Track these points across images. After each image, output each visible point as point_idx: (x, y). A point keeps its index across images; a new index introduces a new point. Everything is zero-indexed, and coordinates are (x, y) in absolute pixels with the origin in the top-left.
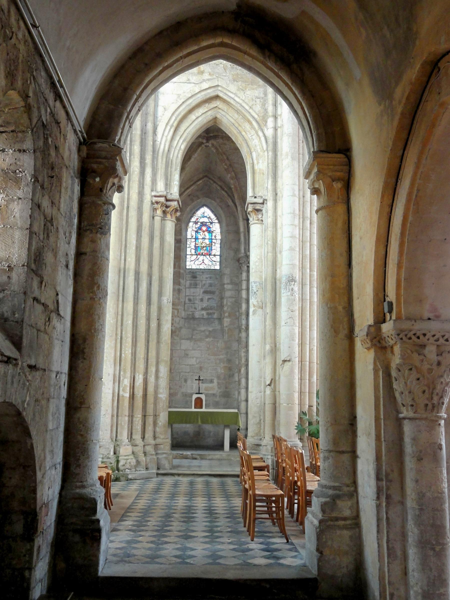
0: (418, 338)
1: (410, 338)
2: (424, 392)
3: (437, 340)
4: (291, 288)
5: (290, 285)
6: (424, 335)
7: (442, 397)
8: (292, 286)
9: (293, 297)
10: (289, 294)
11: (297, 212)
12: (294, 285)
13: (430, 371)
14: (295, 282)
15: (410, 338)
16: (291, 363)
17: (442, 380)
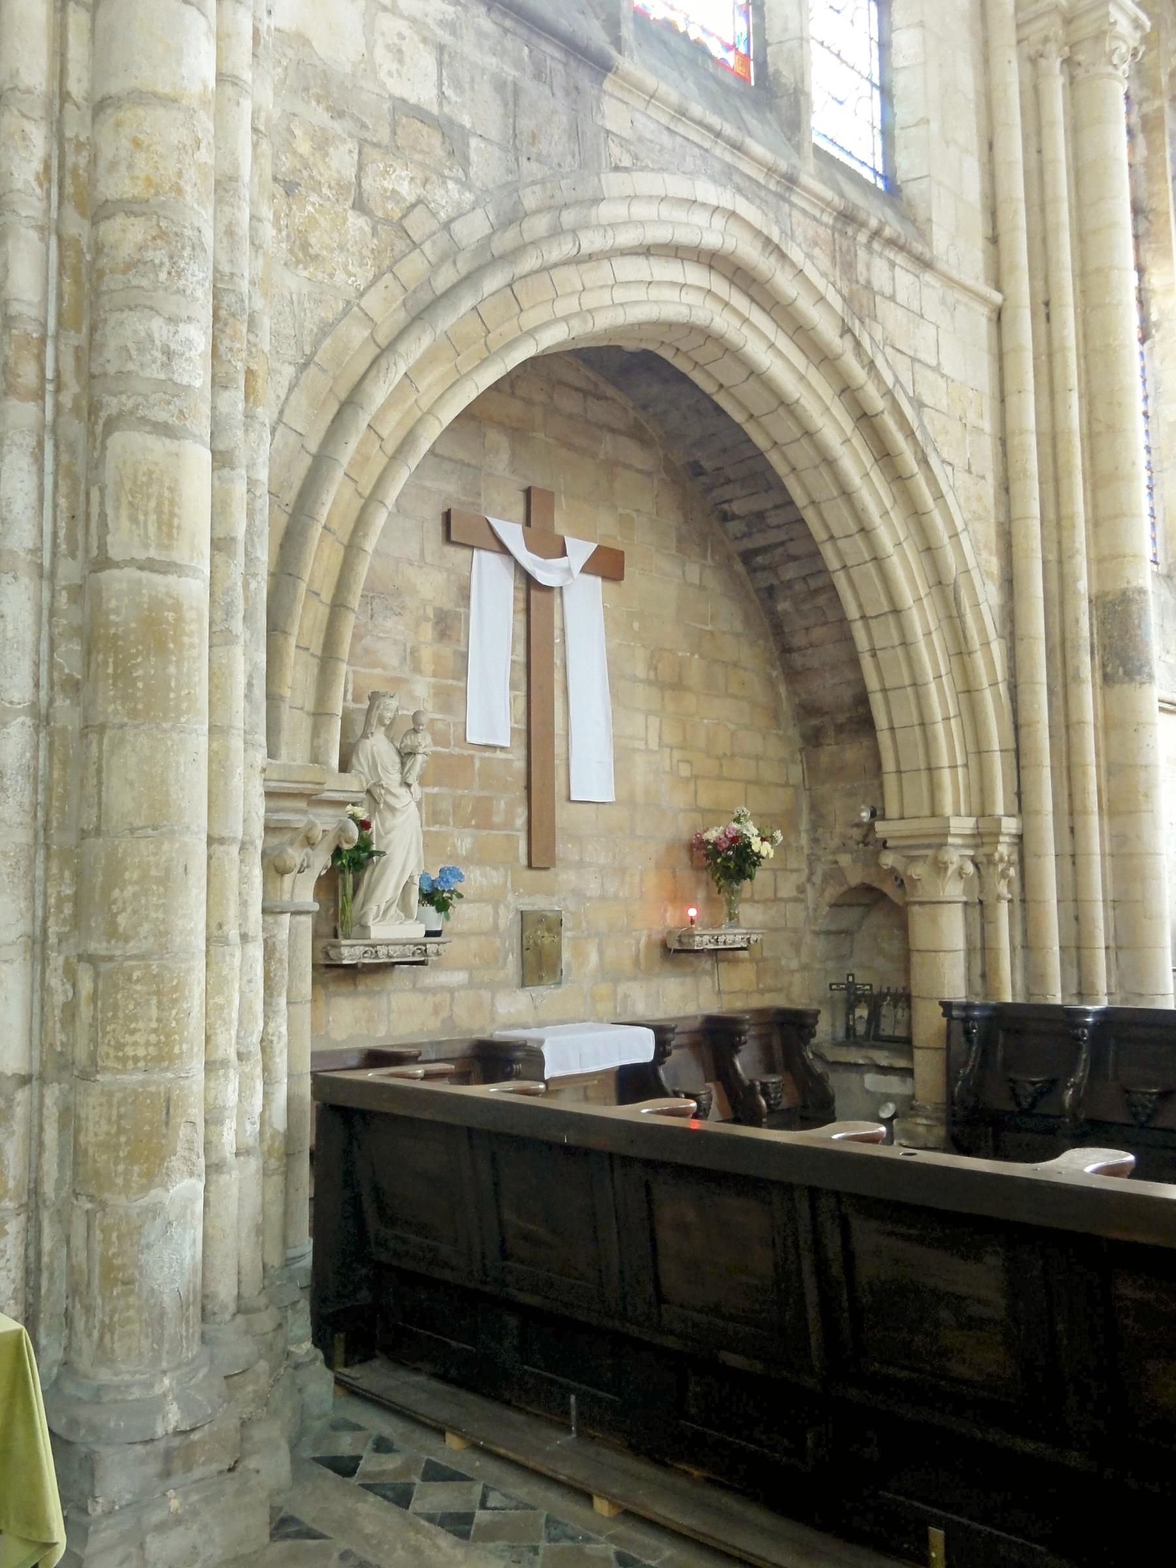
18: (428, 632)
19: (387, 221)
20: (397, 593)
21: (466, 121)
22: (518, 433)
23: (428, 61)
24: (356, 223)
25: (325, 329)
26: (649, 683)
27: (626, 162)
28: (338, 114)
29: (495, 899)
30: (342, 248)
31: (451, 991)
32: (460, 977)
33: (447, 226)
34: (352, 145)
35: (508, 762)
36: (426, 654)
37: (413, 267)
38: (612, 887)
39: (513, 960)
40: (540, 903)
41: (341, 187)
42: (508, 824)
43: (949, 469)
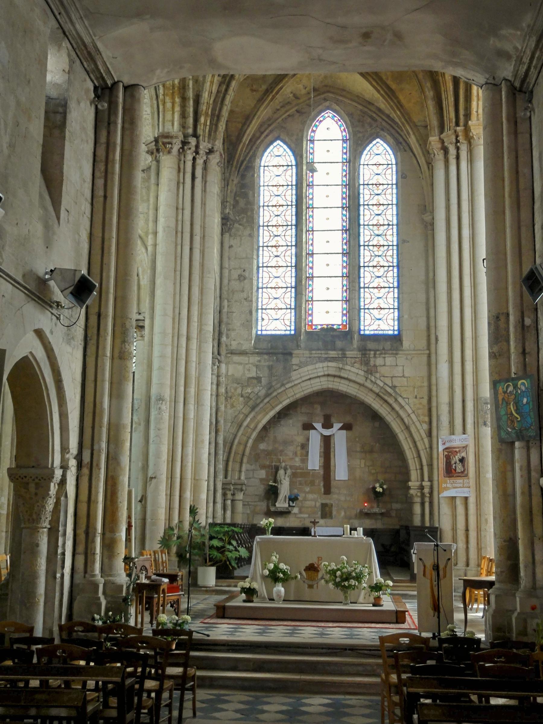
0: (22, 478)
1: (17, 479)
2: (27, 512)
3: (34, 480)
4: (158, 406)
5: (158, 404)
6: (26, 477)
7: (39, 515)
8: (160, 405)
9: (160, 416)
10: (157, 412)
11: (170, 331)
12: (162, 404)
13: (31, 498)
14: (163, 400)
15: (17, 479)
16: (156, 480)
17: (38, 504)
18: (299, 448)
19: (247, 397)
20: (292, 442)
21: (261, 376)
22: (323, 404)
23: (255, 369)
24: (241, 399)
25: (236, 416)
26: (362, 452)
27: (297, 368)
28: (238, 384)
29: (315, 500)
30: (239, 404)
31: (304, 518)
32: (306, 516)
33: (257, 394)
34: (241, 388)
35: (319, 473)
36: (299, 453)
37: (251, 403)
38: (348, 499)
39: (320, 513)
40: (328, 501)
41: (239, 395)
42: (319, 485)
43: (407, 400)
